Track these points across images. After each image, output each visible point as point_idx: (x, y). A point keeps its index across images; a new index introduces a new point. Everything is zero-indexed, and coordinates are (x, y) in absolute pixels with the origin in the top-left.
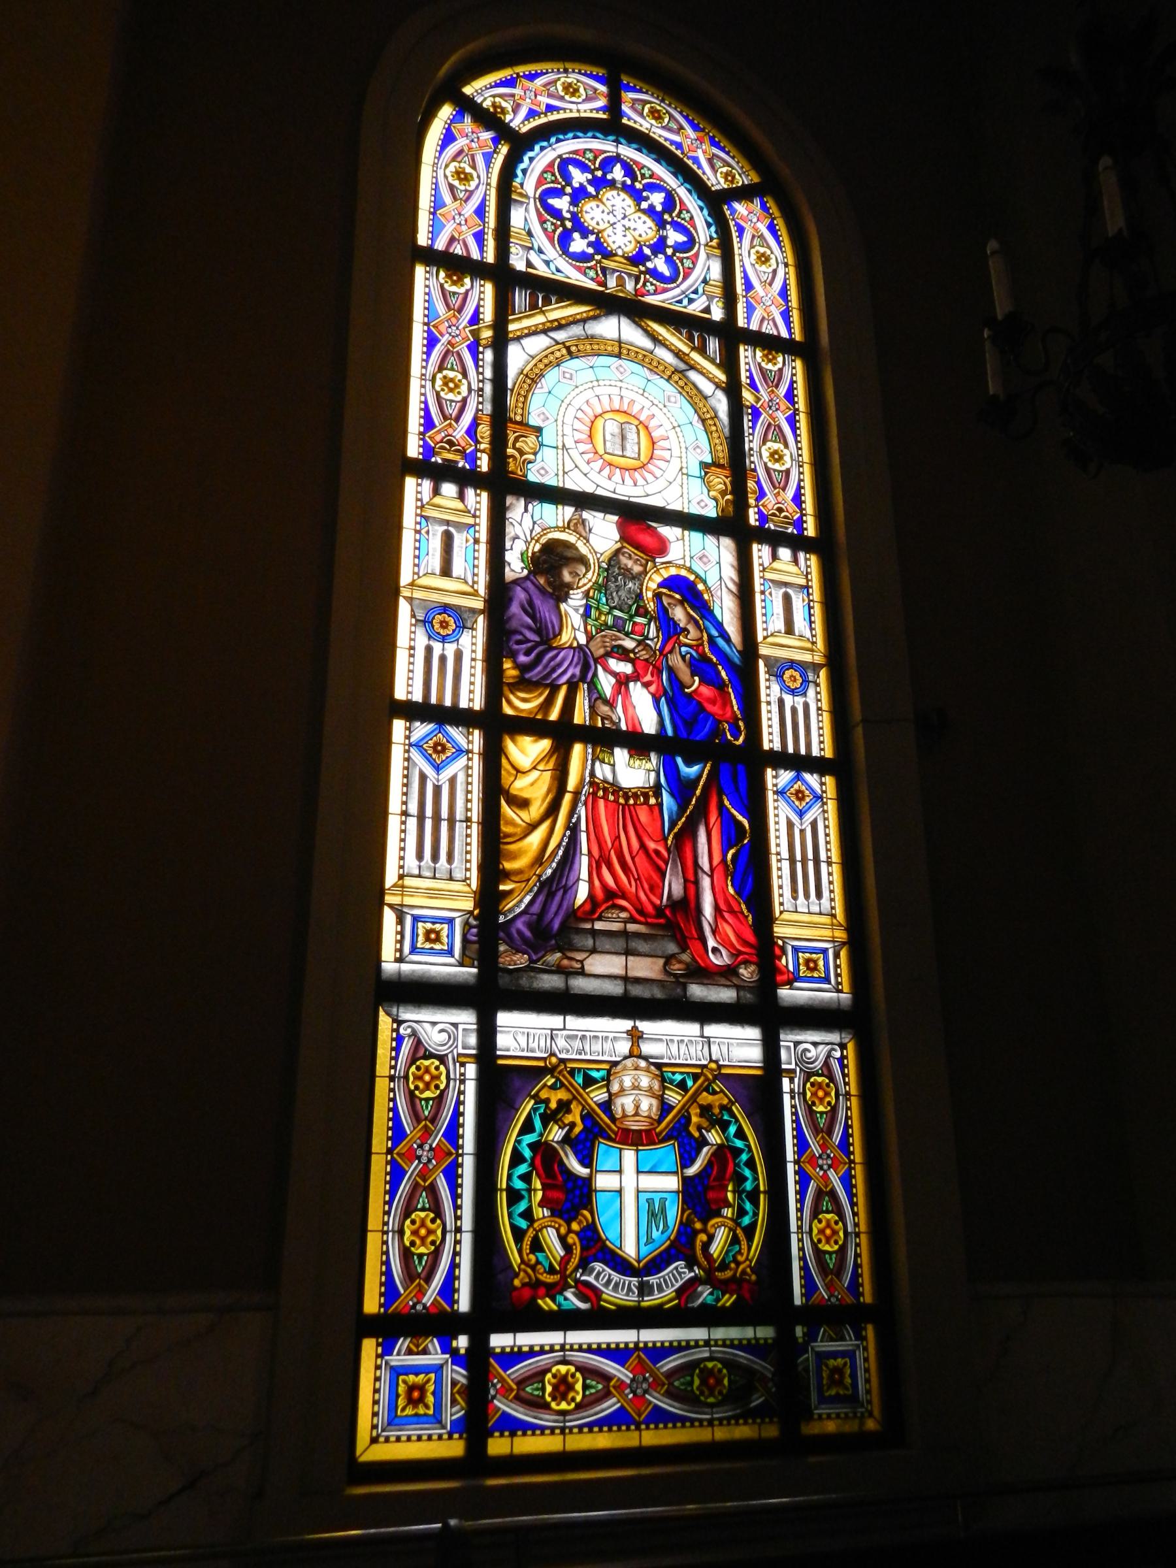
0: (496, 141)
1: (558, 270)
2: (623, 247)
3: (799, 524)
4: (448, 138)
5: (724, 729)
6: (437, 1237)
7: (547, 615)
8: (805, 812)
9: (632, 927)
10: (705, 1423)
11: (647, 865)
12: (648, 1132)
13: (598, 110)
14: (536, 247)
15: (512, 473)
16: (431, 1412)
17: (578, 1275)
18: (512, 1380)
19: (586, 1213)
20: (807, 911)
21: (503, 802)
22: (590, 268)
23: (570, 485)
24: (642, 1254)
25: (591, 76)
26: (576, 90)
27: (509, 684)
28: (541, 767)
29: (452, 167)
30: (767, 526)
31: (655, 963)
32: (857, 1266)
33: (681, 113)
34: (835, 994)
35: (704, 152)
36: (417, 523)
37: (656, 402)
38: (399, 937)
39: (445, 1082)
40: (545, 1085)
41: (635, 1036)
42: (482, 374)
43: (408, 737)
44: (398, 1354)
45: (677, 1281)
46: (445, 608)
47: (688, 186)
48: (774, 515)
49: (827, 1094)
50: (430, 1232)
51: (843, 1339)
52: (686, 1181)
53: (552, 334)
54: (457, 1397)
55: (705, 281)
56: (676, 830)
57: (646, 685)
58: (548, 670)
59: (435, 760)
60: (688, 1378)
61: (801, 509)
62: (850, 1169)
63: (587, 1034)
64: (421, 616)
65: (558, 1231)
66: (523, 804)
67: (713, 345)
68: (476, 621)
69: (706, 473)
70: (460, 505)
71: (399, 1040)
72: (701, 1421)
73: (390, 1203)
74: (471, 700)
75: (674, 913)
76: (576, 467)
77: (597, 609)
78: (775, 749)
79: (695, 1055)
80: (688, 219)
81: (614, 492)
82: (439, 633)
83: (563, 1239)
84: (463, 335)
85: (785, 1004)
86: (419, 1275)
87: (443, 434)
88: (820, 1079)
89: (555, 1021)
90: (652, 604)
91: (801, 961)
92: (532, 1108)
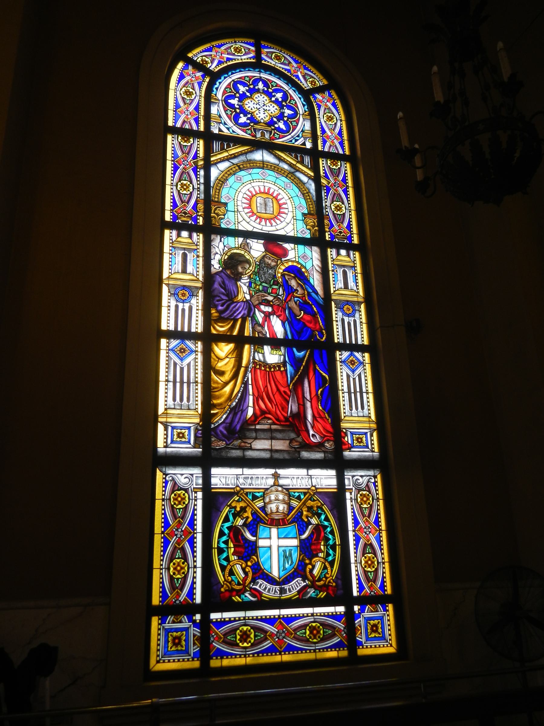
0: (203, 76)
1: (233, 132)
2: (264, 118)
3: (350, 238)
4: (181, 77)
5: (316, 334)
6: (185, 570)
7: (231, 287)
9: (274, 427)
10: (312, 651)
11: (280, 398)
13: (250, 58)
14: (223, 122)
15: (214, 224)
16: (184, 649)
17: (251, 585)
18: (221, 634)
19: (254, 557)
20: (357, 415)
21: (212, 373)
22: (248, 129)
23: (241, 228)
24: (281, 575)
25: (247, 43)
26: (241, 50)
27: (214, 320)
28: (230, 356)
29: (183, 90)
30: (334, 240)
31: (285, 443)
32: (383, 577)
33: (290, 56)
34: (371, 453)
35: (301, 73)
36: (170, 250)
37: (281, 187)
38: (165, 436)
40: (234, 500)
41: (276, 476)
42: (199, 181)
43: (168, 347)
44: (168, 623)
45: (298, 587)
46: (184, 287)
47: (294, 89)
48: (337, 235)
49: (368, 499)
50: (182, 568)
51: (377, 611)
52: (301, 541)
53: (231, 161)
54: (196, 641)
56: (294, 382)
57: (278, 316)
58: (232, 312)
59: (180, 356)
60: (304, 631)
61: (351, 231)
62: (380, 533)
65: (241, 565)
66: (221, 373)
67: (307, 159)
68: (198, 292)
69: (305, 218)
70: (190, 241)
71: (166, 482)
72: (310, 650)
73: (163, 556)
74: (197, 328)
75: (293, 419)
76: (244, 219)
77: (255, 283)
78: (340, 342)
79: (305, 483)
80: (294, 103)
81: (262, 230)
82: (181, 299)
83: (244, 570)
85: (347, 459)
86: (177, 588)
87: (181, 209)
88: (364, 492)
89: (239, 471)
90: (280, 279)
91: (354, 438)
92: (228, 511)
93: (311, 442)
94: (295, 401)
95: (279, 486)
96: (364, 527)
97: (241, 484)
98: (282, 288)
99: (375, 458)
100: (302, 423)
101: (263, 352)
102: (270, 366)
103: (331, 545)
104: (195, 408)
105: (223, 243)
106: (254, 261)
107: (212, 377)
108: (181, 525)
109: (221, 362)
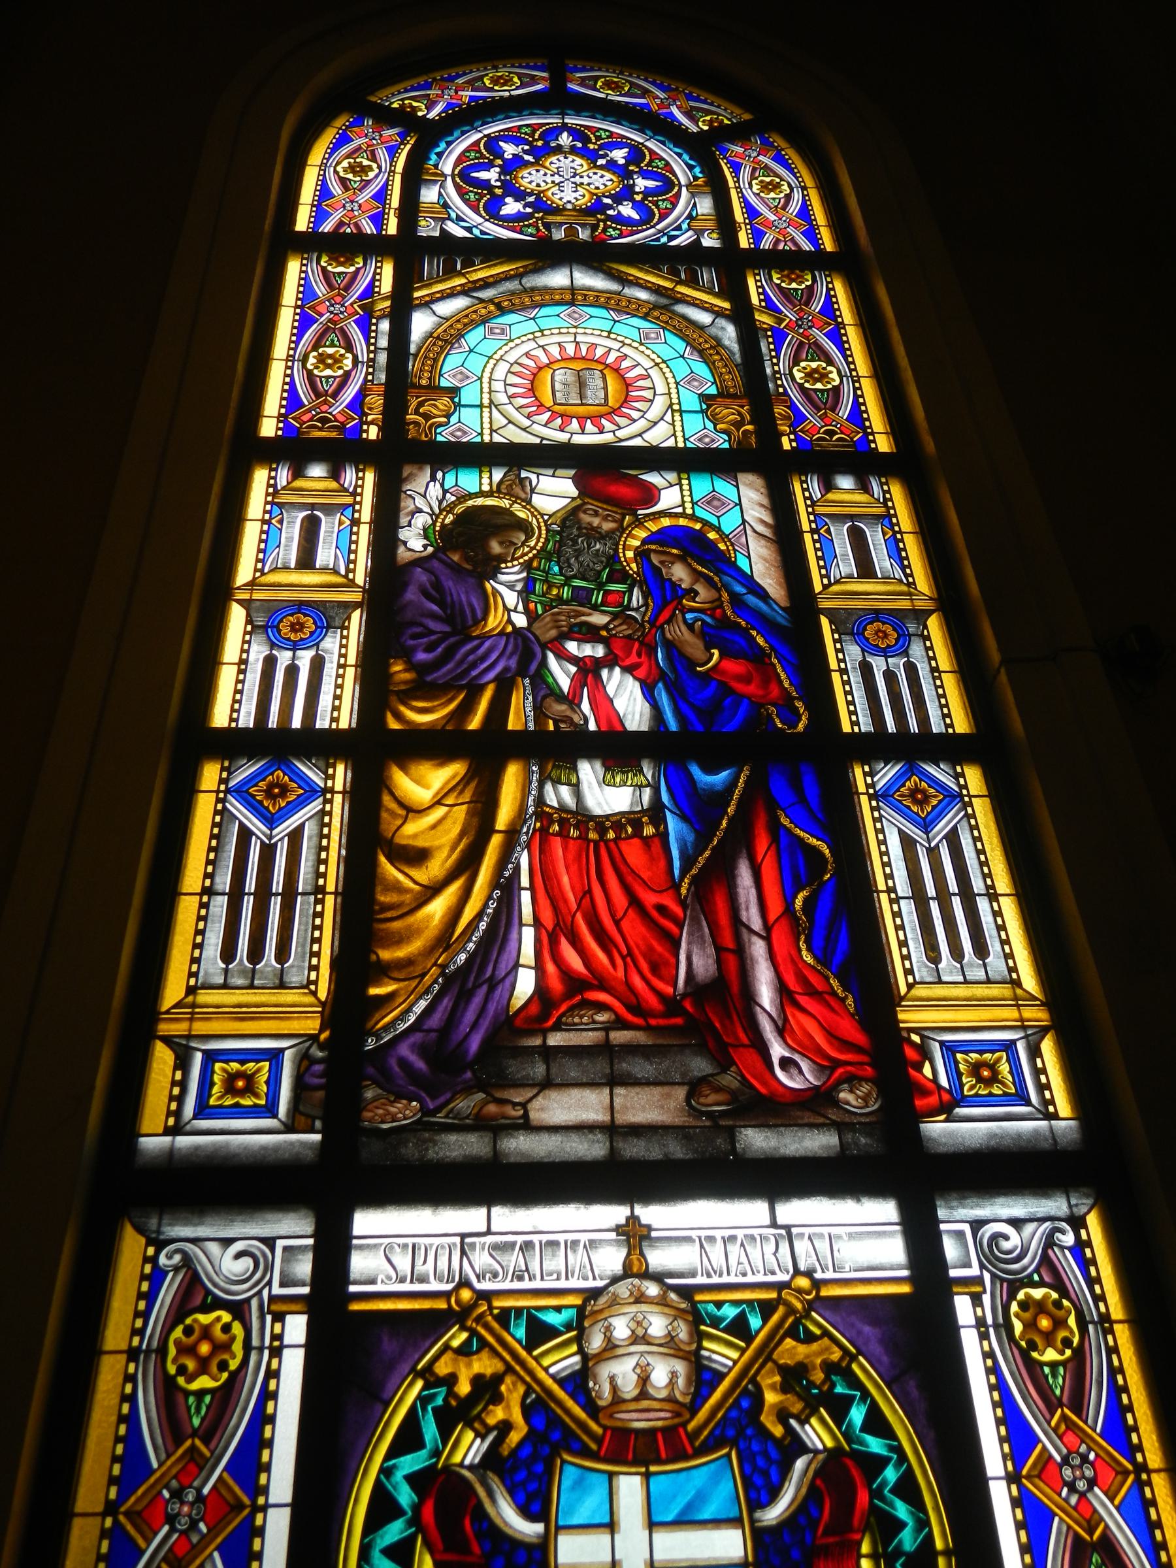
0: (403, 136)
5: (769, 716)
8: (932, 821)
9: (619, 1037)
11: (643, 930)
12: (669, 1432)
20: (961, 979)
21: (382, 859)
26: (511, 80)
27: (397, 693)
28: (450, 801)
31: (668, 1096)
33: (646, 80)
34: (1044, 1123)
35: (678, 107)
36: (265, 512)
37: (628, 341)
39: (240, 1354)
40: (447, 1347)
46: (301, 606)
49: (1059, 1323)
52: (761, 1537)
53: (475, 294)
55: (690, 217)
56: (694, 871)
57: (628, 670)
58: (465, 666)
59: (267, 808)
61: (864, 428)
62: (1140, 1485)
63: (536, 1238)
64: (260, 620)
66: (418, 856)
68: (349, 618)
69: (709, 406)
70: (334, 485)
76: (510, 422)
77: (546, 581)
82: (289, 639)
84: (350, 311)
85: (942, 1149)
88: (1038, 1293)
89: (471, 1218)
90: (634, 566)
91: (962, 1067)
92: (419, 1397)
93: (781, 1089)
94: (702, 937)
95: (647, 1275)
96: (1058, 1458)
97: (478, 1277)
98: (641, 588)
99: (1063, 1142)
100: (735, 1017)
101: (574, 781)
102: (602, 823)
103: (909, 1556)
104: (305, 982)
105: (442, 485)
106: (542, 524)
107: (379, 870)
108: (201, 1469)
109: (413, 818)
